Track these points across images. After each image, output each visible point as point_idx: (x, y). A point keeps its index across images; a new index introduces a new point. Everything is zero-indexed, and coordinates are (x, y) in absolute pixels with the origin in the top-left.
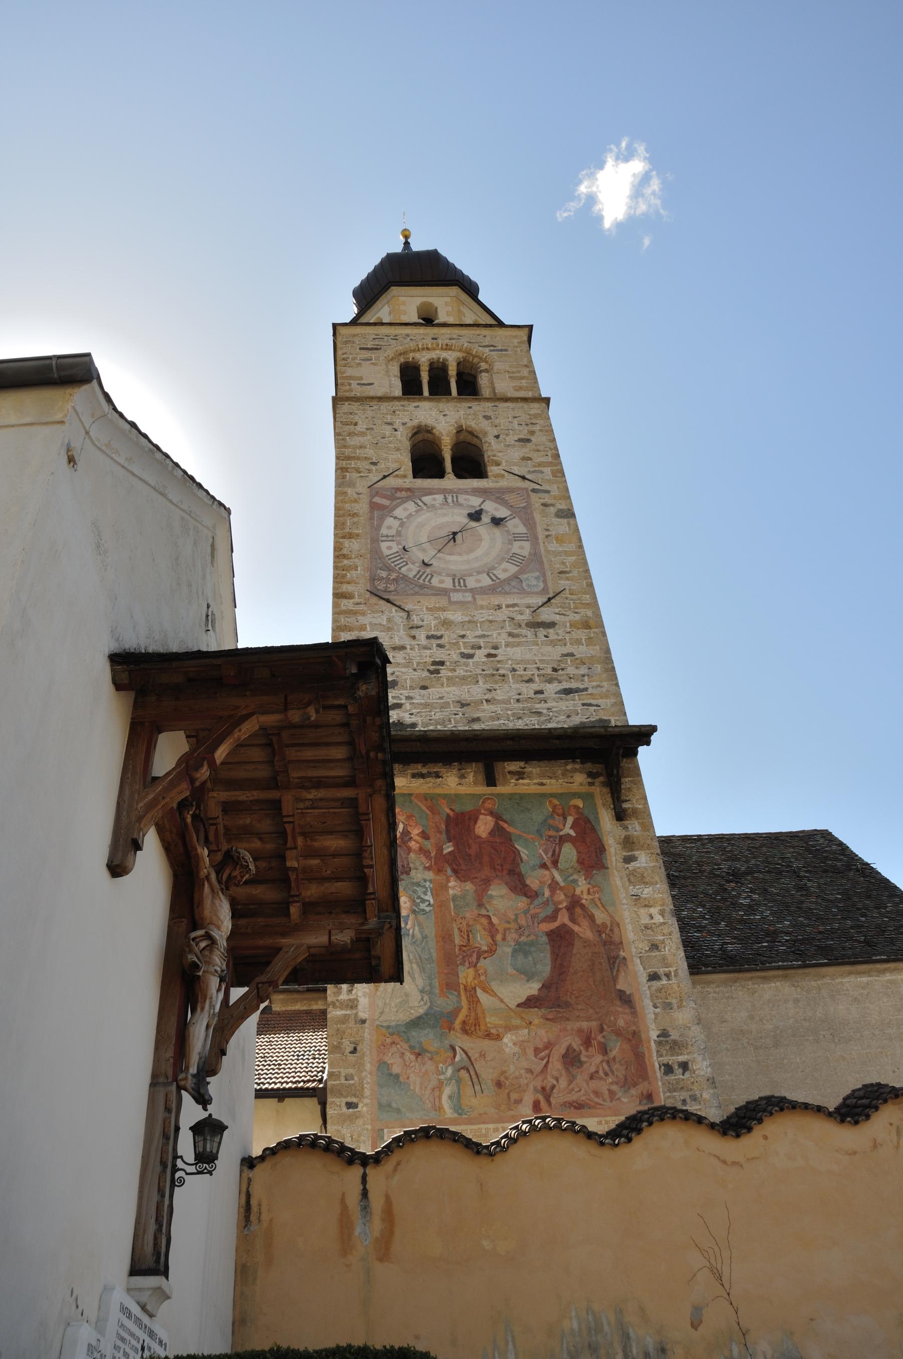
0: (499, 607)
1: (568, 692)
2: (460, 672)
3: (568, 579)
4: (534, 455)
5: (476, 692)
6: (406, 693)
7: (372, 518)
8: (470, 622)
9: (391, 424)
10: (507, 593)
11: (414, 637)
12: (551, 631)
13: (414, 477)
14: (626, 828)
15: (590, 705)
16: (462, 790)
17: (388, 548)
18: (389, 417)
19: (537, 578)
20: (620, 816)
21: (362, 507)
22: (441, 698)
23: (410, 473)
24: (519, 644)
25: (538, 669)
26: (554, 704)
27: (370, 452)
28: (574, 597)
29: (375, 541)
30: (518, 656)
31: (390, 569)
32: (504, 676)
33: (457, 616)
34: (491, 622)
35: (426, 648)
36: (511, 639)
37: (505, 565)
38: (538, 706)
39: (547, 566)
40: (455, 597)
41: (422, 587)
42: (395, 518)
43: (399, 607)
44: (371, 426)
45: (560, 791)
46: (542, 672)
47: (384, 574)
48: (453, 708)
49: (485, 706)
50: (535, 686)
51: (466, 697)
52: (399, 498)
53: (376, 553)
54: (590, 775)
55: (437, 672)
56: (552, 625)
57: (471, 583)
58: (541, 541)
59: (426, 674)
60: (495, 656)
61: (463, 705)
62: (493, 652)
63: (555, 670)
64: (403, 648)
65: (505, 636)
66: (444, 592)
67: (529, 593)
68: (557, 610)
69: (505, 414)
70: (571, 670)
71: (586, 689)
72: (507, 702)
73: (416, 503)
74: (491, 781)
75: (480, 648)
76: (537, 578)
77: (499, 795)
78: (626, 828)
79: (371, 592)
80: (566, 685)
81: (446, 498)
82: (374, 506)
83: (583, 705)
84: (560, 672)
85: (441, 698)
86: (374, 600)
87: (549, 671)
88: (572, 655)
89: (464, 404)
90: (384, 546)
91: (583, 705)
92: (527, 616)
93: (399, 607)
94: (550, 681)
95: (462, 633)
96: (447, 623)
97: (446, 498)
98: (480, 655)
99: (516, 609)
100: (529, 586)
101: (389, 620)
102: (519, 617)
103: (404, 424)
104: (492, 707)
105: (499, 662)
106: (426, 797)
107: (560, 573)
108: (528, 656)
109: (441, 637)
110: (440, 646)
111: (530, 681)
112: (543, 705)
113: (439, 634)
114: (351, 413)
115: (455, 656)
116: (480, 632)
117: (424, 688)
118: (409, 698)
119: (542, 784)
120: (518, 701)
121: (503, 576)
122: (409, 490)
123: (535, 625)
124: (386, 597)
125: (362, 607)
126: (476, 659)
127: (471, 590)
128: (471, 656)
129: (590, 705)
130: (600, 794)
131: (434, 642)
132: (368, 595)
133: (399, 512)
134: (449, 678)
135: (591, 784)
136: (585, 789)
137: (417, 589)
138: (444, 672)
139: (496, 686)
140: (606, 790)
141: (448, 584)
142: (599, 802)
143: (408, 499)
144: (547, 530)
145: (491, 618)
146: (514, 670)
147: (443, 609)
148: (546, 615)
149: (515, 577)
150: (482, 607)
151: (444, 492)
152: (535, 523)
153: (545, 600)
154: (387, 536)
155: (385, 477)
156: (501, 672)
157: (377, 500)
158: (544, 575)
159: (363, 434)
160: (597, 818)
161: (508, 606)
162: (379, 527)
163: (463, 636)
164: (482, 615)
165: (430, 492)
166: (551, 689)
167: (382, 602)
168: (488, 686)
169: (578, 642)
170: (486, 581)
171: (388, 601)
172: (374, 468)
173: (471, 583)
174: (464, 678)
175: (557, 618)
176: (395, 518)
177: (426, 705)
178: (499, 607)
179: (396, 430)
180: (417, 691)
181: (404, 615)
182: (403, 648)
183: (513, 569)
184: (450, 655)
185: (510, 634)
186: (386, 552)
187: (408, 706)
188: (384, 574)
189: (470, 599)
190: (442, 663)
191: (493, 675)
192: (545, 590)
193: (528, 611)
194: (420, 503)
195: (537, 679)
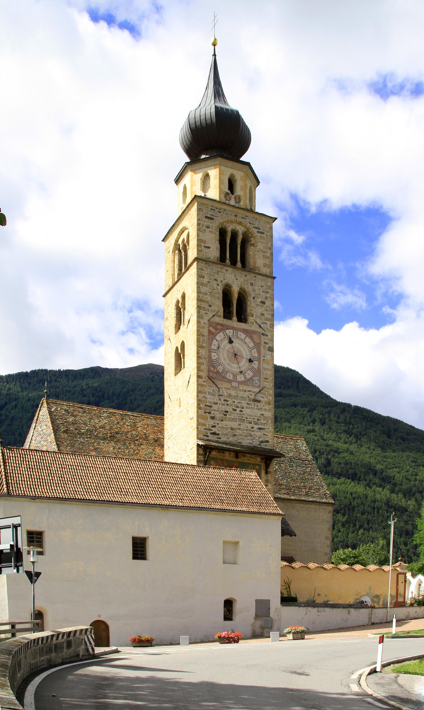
0: (245, 391)
1: (260, 429)
2: (232, 417)
3: (267, 382)
4: (265, 313)
5: (235, 425)
6: (217, 422)
7: (209, 339)
8: (236, 396)
9: (216, 280)
10: (249, 385)
11: (220, 400)
12: (259, 404)
13: (224, 317)
14: (267, 476)
15: (265, 435)
16: (230, 459)
17: (214, 356)
18: (216, 275)
19: (258, 380)
20: (267, 473)
21: (205, 332)
22: (226, 425)
23: (222, 317)
24: (249, 408)
25: (253, 419)
26: (256, 433)
27: (208, 298)
28: (267, 390)
29: (210, 351)
30: (248, 413)
31: (214, 367)
32: (244, 420)
33: (233, 393)
34: (242, 397)
35: (224, 405)
36: (247, 406)
37: (249, 372)
38: (251, 433)
39: (261, 375)
40: (234, 384)
41: (224, 377)
42: (217, 340)
43: (216, 385)
44: (209, 280)
45: (254, 463)
46: (254, 420)
47: (212, 369)
48: (229, 430)
49: (238, 431)
50: (252, 425)
51: (233, 427)
52: (218, 329)
53: (210, 357)
54: (262, 459)
55: (225, 415)
56: (259, 401)
57: (239, 379)
58: (261, 362)
59: (223, 415)
60: (242, 411)
61: (232, 429)
62: (242, 410)
63: (258, 420)
64: (217, 404)
65: (246, 403)
66: (230, 381)
67: (255, 386)
68: (262, 395)
69: (260, 282)
70: (262, 421)
71: (265, 429)
72: (243, 430)
73: (224, 333)
74: (237, 457)
75: (238, 407)
76: (258, 380)
77: (238, 462)
78: (267, 476)
79: (208, 377)
80: (260, 426)
81: (233, 333)
82: (210, 332)
83: (264, 434)
84: (259, 421)
85: (226, 425)
86: (209, 381)
87: (256, 420)
88: (263, 415)
89: (244, 272)
90: (213, 354)
91: (264, 434)
92: (252, 397)
93: (216, 385)
94: (256, 424)
95: (234, 400)
96: (230, 395)
97: (233, 333)
98: (238, 410)
99: (250, 393)
100: (255, 383)
101: (213, 391)
102: (250, 397)
103: (221, 282)
104: (240, 431)
105: (243, 414)
106: (221, 459)
107: (265, 378)
108: (251, 414)
109: (227, 401)
110: (227, 405)
111: (251, 423)
112: (253, 433)
113: (227, 399)
114: (202, 269)
115: (231, 410)
116: (239, 401)
117: (222, 421)
118: (218, 424)
119: (249, 460)
120: (247, 430)
121: (248, 377)
122: (222, 325)
123: (255, 401)
124: (213, 380)
125: (205, 383)
126: (237, 412)
127: (238, 382)
128: (235, 410)
129: (265, 435)
130: (263, 465)
131: (226, 403)
132: (207, 378)
133: (218, 337)
134: (229, 418)
135: (261, 462)
136: (259, 463)
137: (222, 378)
138: (228, 416)
139: (241, 424)
140: (265, 464)
141: (231, 378)
142: (262, 468)
143: (221, 330)
144: (264, 357)
145: (242, 396)
146: (247, 418)
147: (229, 389)
148: (259, 398)
149: (251, 378)
150: (241, 390)
151: (233, 328)
152: (261, 352)
153: (259, 390)
154: (214, 350)
155: (214, 316)
156: (243, 418)
157: (211, 328)
158: (260, 378)
159: (206, 285)
160: (261, 472)
161: (248, 391)
162: (211, 344)
163: (234, 402)
164: (241, 394)
165: (228, 328)
166: (256, 427)
167: (211, 382)
168: (239, 423)
169: (265, 410)
170: (243, 379)
171: (213, 382)
172: (210, 308)
173: (239, 379)
174: (233, 419)
175: (261, 399)
176: (217, 340)
177: (222, 427)
178: (245, 391)
179: (218, 285)
180: (220, 422)
181: (217, 389)
182: (217, 404)
183: (252, 374)
184: (229, 409)
185: (248, 404)
186: (213, 358)
187: (217, 427)
188: (212, 369)
189: (237, 386)
190: (227, 412)
191: (241, 419)
192: (259, 386)
193: (253, 394)
194: (225, 334)
195: (253, 423)
